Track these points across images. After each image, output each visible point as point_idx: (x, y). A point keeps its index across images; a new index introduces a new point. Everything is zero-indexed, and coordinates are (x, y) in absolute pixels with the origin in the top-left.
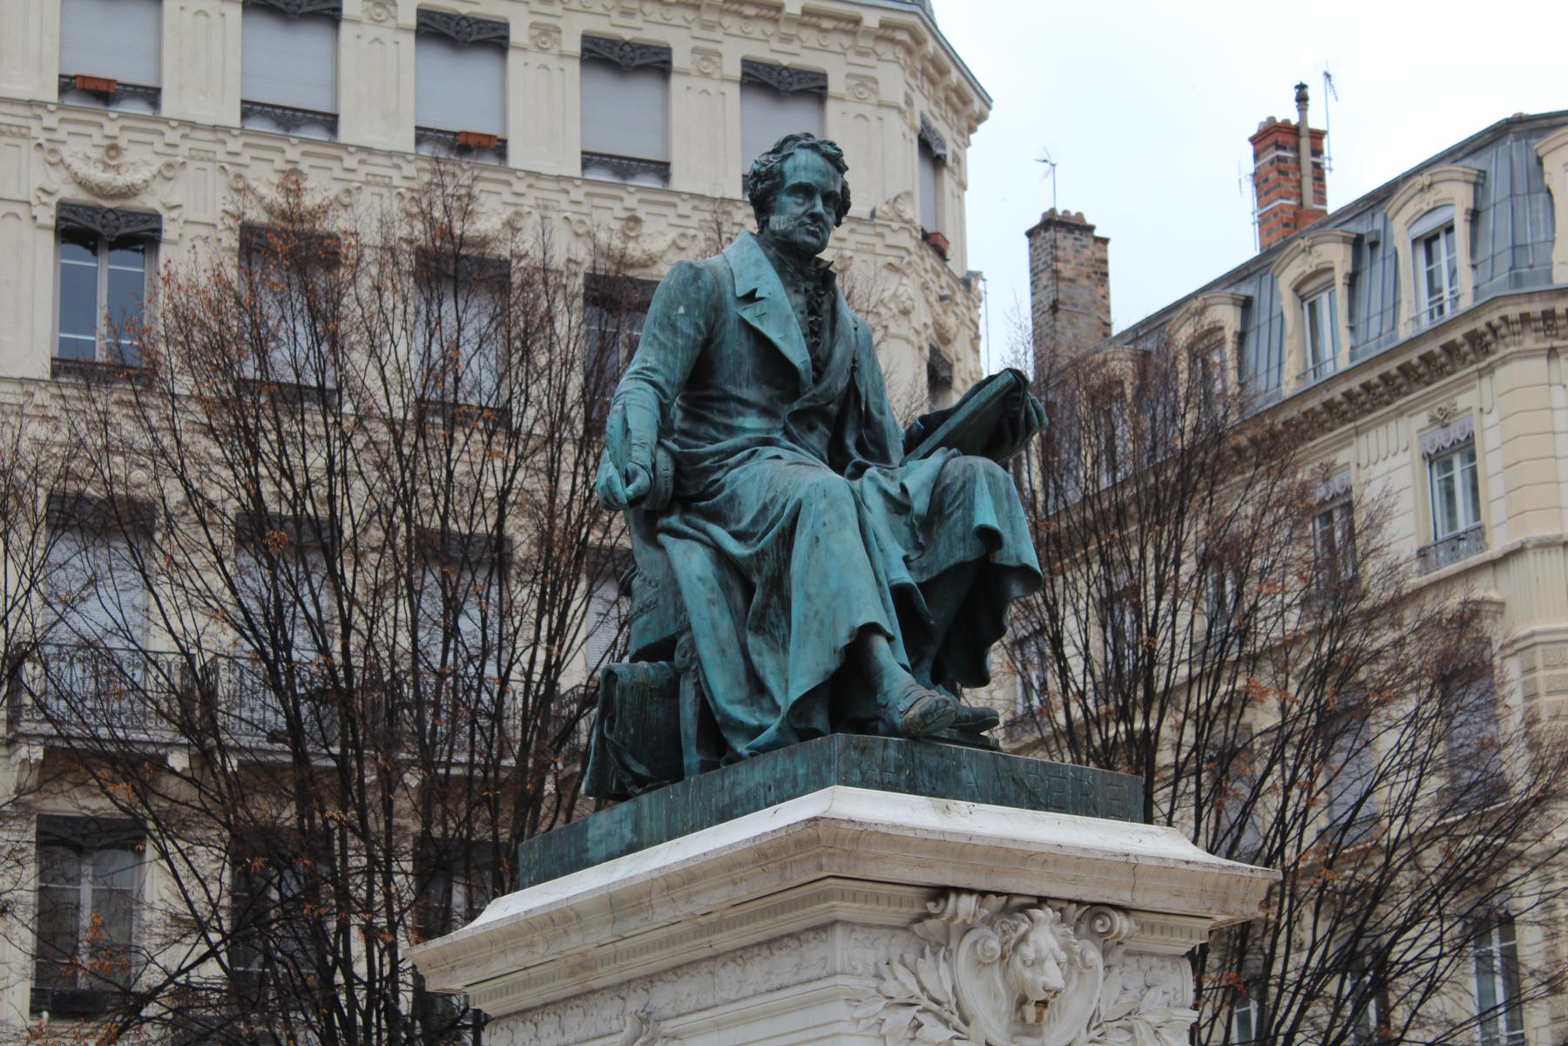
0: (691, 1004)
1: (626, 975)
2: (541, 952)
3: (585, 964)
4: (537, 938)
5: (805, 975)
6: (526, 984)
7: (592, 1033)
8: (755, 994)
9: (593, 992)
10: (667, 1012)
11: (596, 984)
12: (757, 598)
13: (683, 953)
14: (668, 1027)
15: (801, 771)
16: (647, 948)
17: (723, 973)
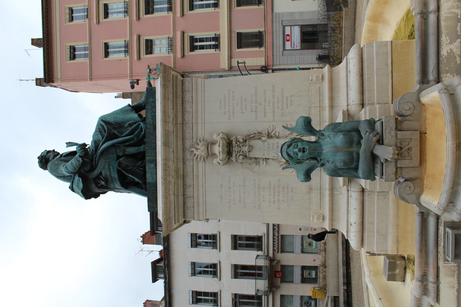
0: (191, 131)
1: (181, 160)
2: (172, 187)
3: (177, 171)
4: (168, 178)
5: (191, 90)
6: (178, 197)
7: (192, 173)
8: (192, 108)
9: (183, 175)
10: (191, 141)
11: (182, 173)
12: (116, 132)
13: (180, 135)
14: (194, 140)
15: (151, 100)
16: (177, 145)
17: (186, 110)
